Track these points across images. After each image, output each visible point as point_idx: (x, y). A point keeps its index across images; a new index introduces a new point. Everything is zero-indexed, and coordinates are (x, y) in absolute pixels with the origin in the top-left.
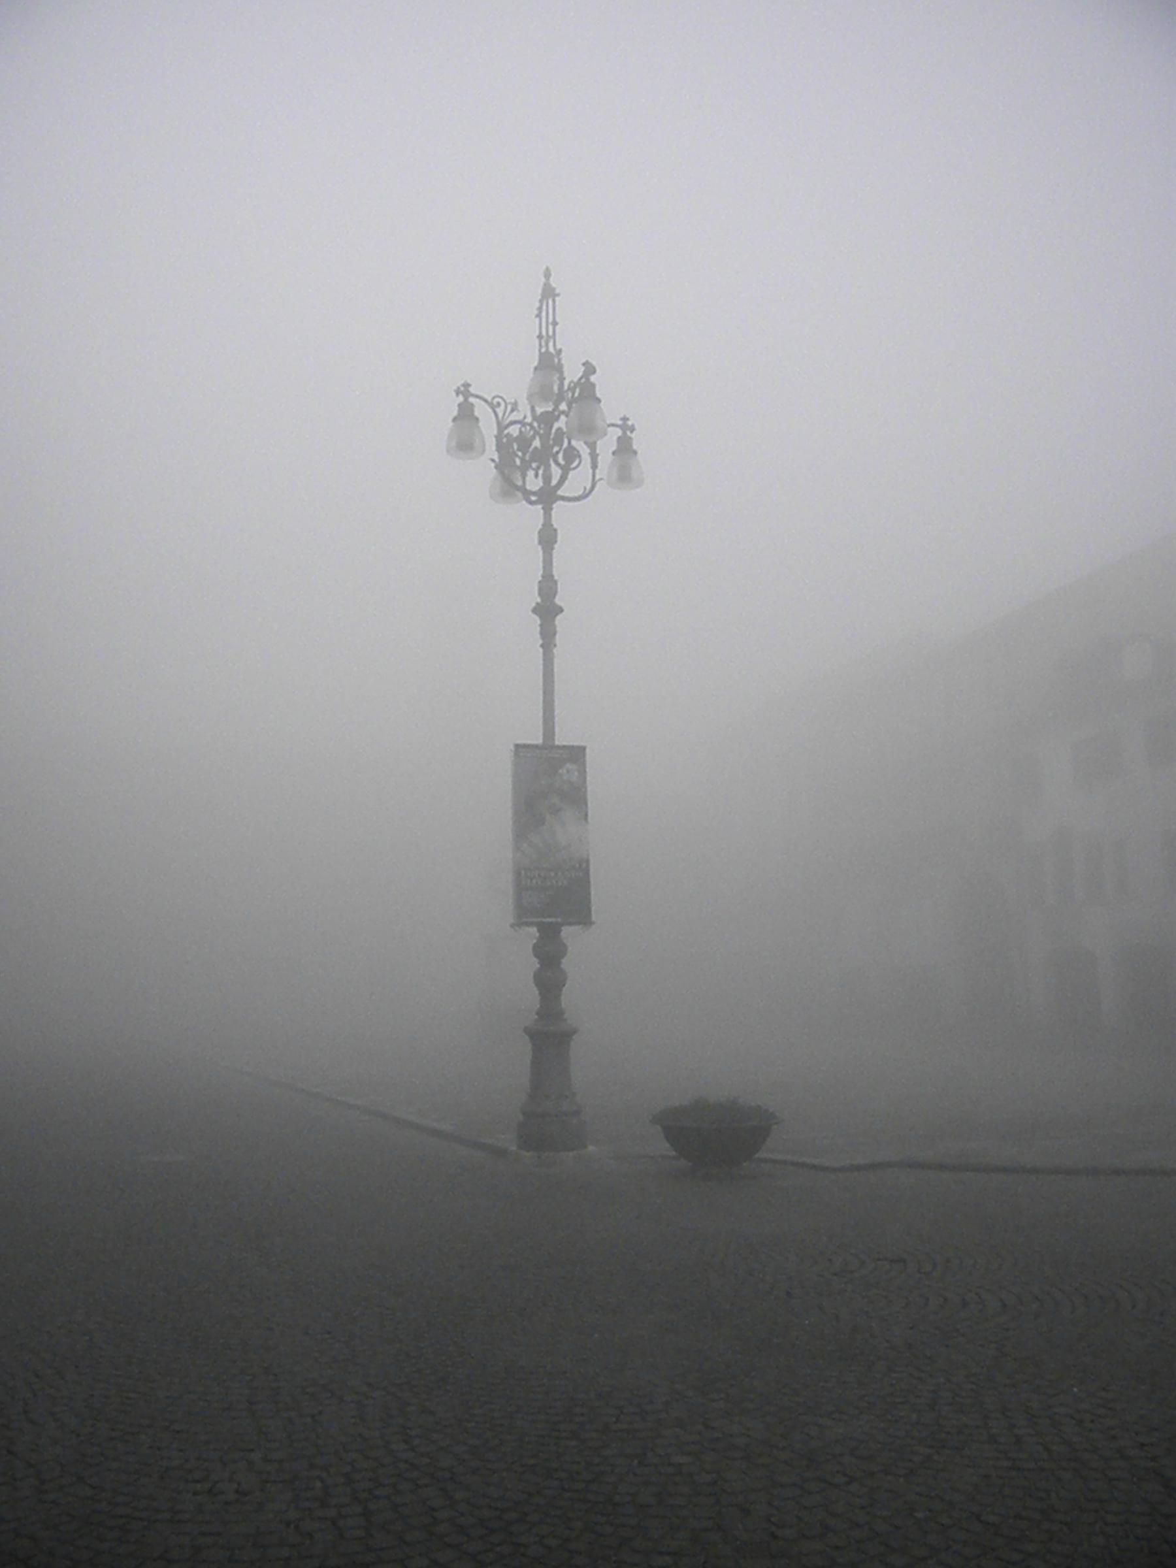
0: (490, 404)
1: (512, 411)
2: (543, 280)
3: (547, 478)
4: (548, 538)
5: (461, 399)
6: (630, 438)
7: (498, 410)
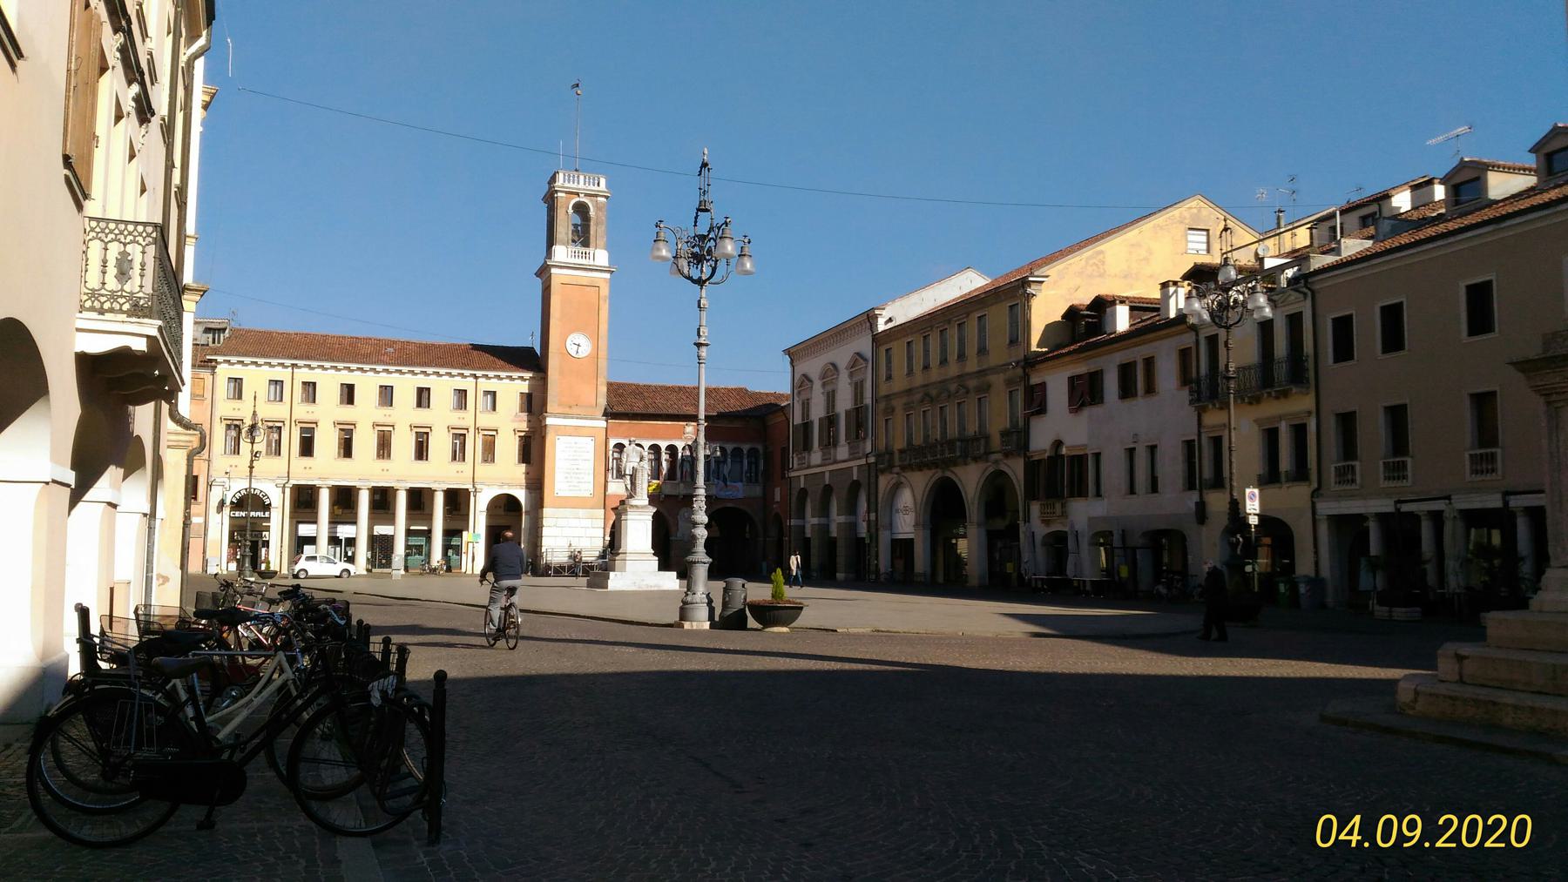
3: (702, 271)
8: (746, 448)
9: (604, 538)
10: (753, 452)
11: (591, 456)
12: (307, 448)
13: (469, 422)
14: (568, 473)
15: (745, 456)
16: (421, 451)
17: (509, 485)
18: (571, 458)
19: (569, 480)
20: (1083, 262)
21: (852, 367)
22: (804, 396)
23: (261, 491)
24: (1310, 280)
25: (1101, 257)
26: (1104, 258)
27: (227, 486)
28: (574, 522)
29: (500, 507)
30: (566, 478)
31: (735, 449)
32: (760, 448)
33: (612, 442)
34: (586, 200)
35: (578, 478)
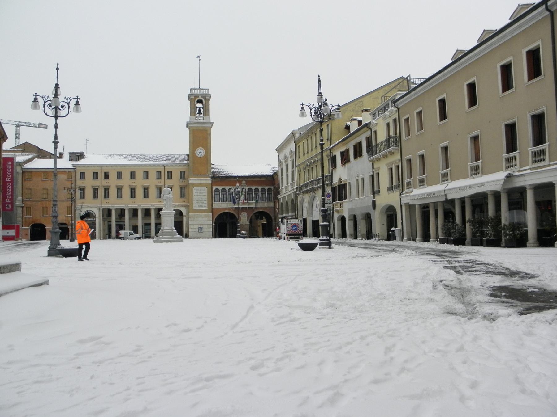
0: (42, 98)
1: (48, 98)
2: (57, 66)
4: (56, 127)
5: (35, 97)
6: (79, 101)
7: (44, 98)
8: (266, 188)
9: (212, 224)
10: (269, 190)
11: (206, 194)
12: (107, 195)
13: (162, 183)
14: (197, 201)
15: (266, 191)
16: (146, 195)
17: (178, 206)
18: (199, 195)
19: (198, 203)
20: (354, 106)
21: (291, 154)
22: (281, 167)
23: (92, 211)
24: (396, 104)
25: (362, 103)
26: (363, 104)
27: (81, 209)
28: (200, 219)
29: (178, 214)
30: (197, 202)
31: (255, 189)
32: (272, 188)
33: (214, 188)
34: (202, 99)
35: (201, 202)
